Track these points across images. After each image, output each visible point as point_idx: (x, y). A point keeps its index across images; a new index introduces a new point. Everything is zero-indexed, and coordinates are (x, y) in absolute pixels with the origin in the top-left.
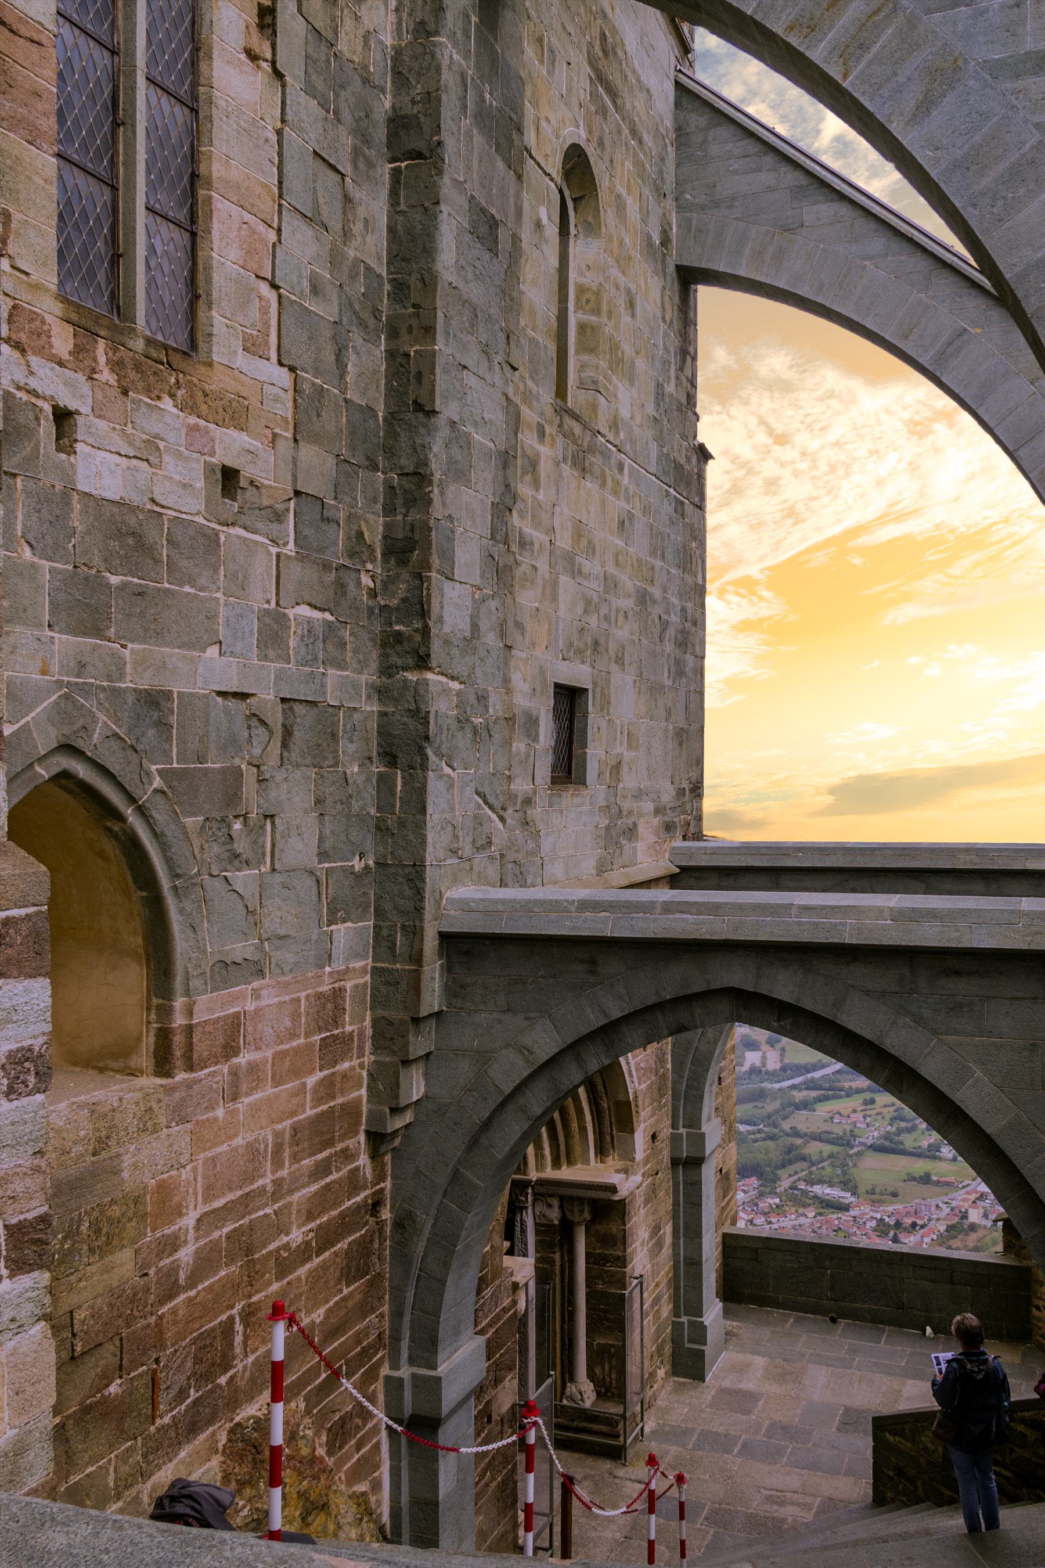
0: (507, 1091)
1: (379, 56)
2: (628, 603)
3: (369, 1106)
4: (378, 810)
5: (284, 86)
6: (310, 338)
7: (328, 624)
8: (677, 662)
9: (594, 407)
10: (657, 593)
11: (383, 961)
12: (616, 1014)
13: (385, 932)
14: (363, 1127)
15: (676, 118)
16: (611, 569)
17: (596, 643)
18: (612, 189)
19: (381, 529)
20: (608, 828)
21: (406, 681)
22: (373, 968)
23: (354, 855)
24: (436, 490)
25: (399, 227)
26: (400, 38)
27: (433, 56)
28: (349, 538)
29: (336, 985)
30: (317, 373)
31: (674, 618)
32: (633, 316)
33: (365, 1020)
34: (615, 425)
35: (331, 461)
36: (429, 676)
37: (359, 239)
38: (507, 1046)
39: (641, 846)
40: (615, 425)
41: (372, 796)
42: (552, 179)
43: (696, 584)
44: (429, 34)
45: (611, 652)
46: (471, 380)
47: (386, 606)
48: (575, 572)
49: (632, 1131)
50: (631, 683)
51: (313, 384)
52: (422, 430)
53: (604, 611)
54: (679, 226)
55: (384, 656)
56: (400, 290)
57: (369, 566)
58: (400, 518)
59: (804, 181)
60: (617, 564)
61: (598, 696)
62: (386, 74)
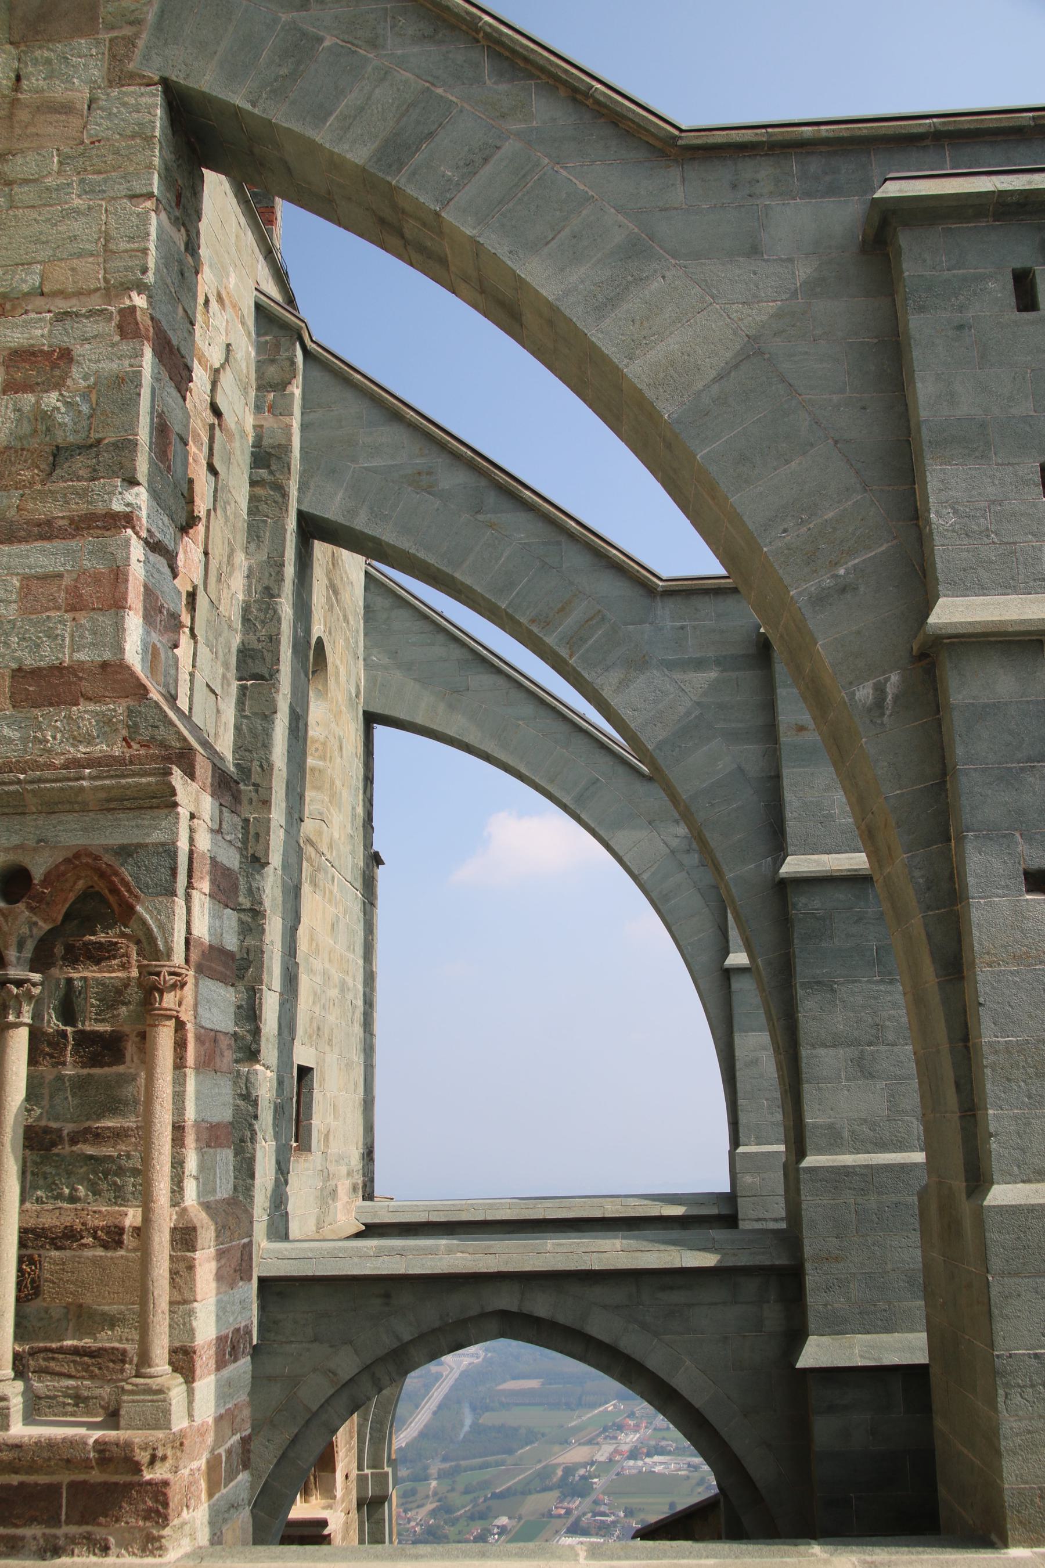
0: (314, 1408)
2: (334, 993)
5: (196, 643)
9: (320, 833)
12: (407, 1337)
16: (327, 965)
17: (319, 1029)
20: (322, 1189)
25: (244, 727)
26: (250, 596)
27: (275, 611)
34: (331, 847)
36: (258, 1067)
38: (315, 1370)
39: (339, 1205)
44: (272, 596)
49: (334, 1470)
52: (257, 877)
53: (323, 1001)
54: (366, 680)
60: (330, 961)
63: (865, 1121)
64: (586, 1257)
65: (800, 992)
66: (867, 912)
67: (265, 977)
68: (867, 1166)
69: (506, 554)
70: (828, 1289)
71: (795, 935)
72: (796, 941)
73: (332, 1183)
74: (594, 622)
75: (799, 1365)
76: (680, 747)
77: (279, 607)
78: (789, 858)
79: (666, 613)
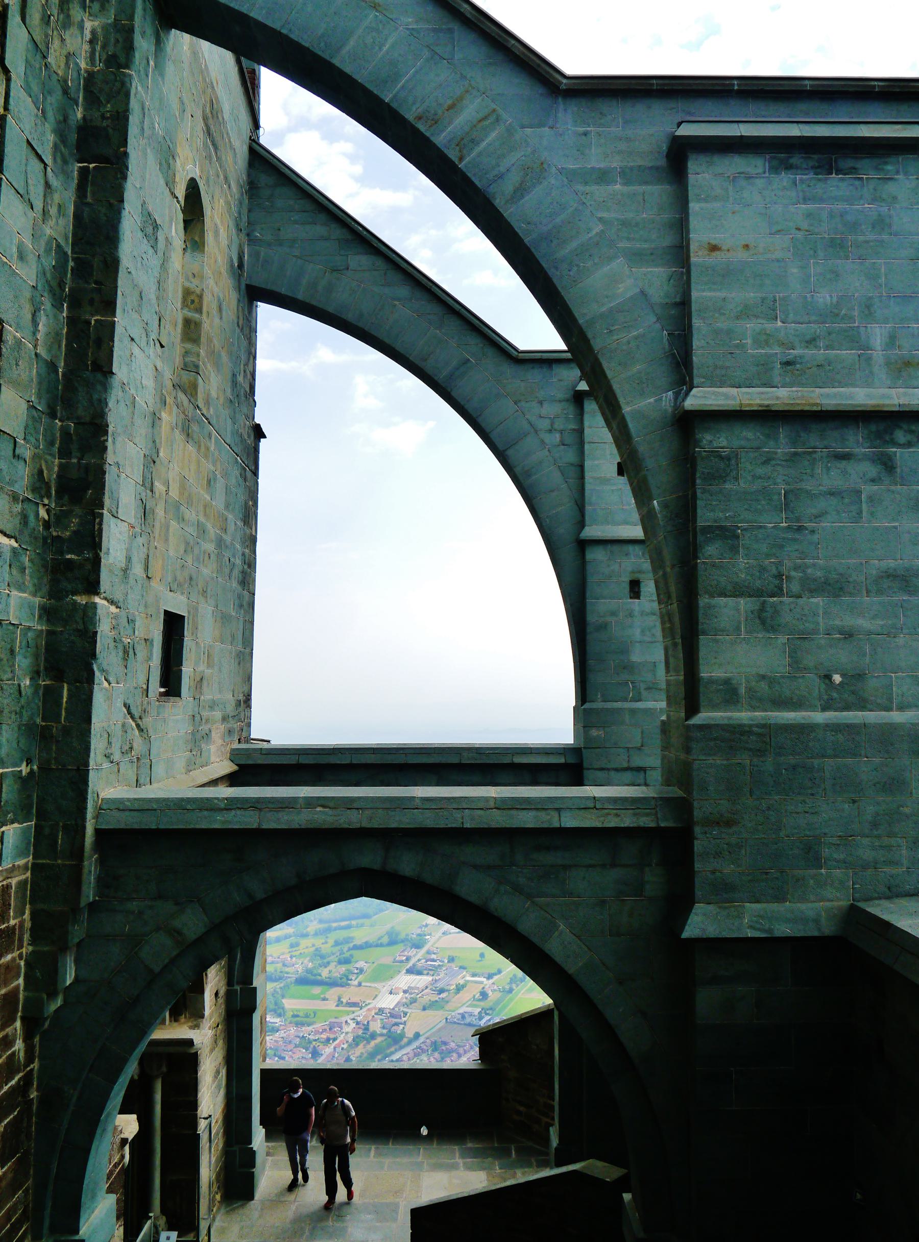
0: (157, 969)
1: (75, 75)
2: (210, 547)
3: (26, 994)
4: (43, 719)
5: (8, 80)
6: (16, 297)
7: (14, 550)
8: (240, 597)
10: (228, 538)
11: (44, 858)
12: (260, 895)
13: (47, 831)
14: (19, 1014)
15: (249, 175)
16: (202, 519)
17: (191, 579)
18: (212, 218)
19: (56, 469)
20: (193, 733)
21: (75, 602)
22: (33, 864)
23: (22, 761)
24: (110, 439)
27: (123, 84)
28: (32, 475)
29: (5, 883)
30: (18, 327)
31: (238, 562)
32: (221, 318)
33: (24, 914)
34: (207, 403)
35: (24, 406)
36: (97, 600)
37: (54, 220)
40: (207, 403)
41: (39, 707)
42: (178, 202)
43: (251, 535)
44: (120, 66)
45: (200, 586)
46: (136, 351)
47: (58, 536)
48: (181, 519)
49: (202, 992)
50: (211, 612)
51: (15, 337)
52: (99, 387)
53: (196, 551)
54: (250, 255)
55: (54, 582)
56: (82, 269)
57: (46, 501)
58: (75, 461)
59: (349, 236)
60: (205, 515)
61: (191, 622)
62: (79, 90)
63: (763, 677)
64: (458, 815)
65: (700, 538)
66: (776, 453)
67: (107, 501)
68: (764, 726)
69: (390, 41)
70: (718, 854)
71: (698, 475)
72: (698, 481)
73: (204, 728)
74: (487, 123)
75: (685, 935)
76: (577, 265)
77: (127, 80)
78: (694, 391)
79: (568, 118)
